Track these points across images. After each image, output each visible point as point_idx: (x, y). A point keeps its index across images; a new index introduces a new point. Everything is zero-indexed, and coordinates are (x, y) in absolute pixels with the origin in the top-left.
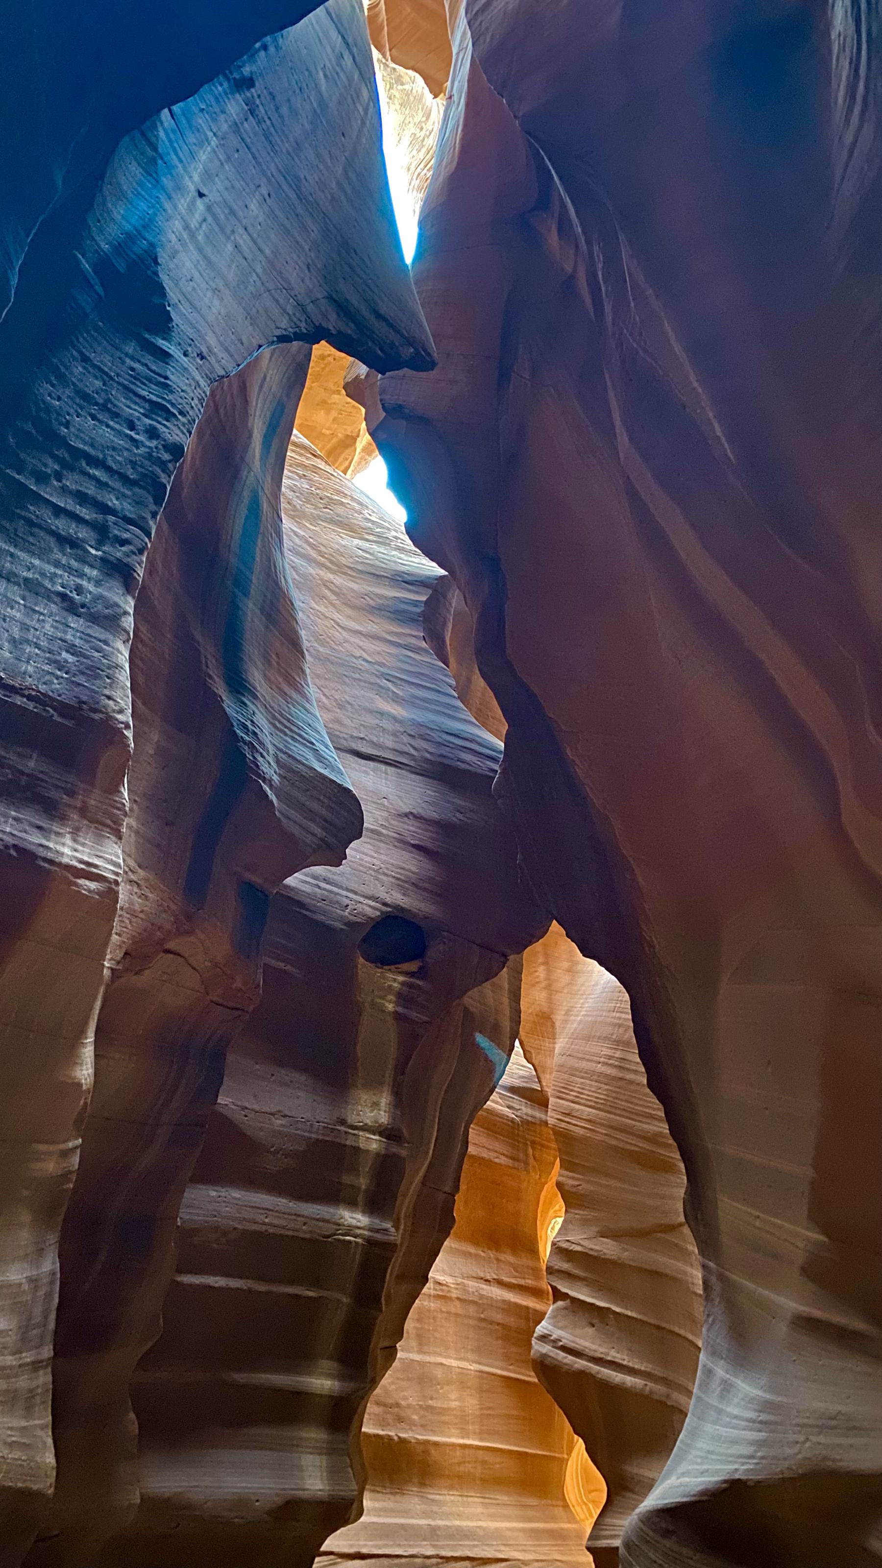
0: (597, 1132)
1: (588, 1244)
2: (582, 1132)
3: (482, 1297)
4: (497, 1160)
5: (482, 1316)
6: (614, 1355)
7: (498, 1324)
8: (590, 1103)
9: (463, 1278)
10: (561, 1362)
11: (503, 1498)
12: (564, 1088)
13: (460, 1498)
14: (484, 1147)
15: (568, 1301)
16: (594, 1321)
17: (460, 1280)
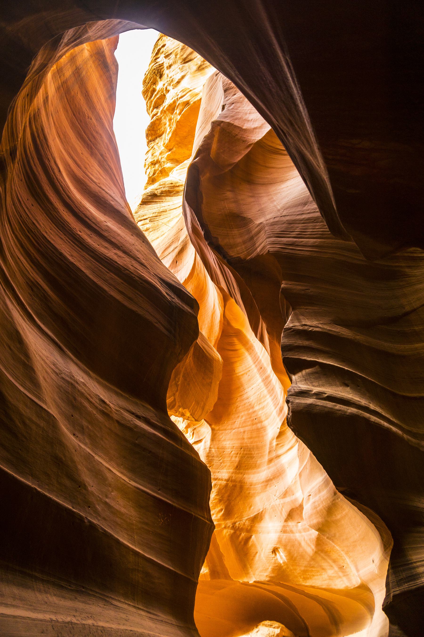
0: (326, 253)
1: (327, 327)
2: (308, 254)
3: (136, 426)
4: (156, 325)
5: (137, 442)
6: (372, 406)
7: (150, 452)
8: (315, 236)
9: (120, 408)
10: (332, 408)
11: (163, 616)
12: (282, 231)
13: (134, 610)
14: (148, 312)
15: (317, 367)
16: (347, 382)
17: (117, 409)
